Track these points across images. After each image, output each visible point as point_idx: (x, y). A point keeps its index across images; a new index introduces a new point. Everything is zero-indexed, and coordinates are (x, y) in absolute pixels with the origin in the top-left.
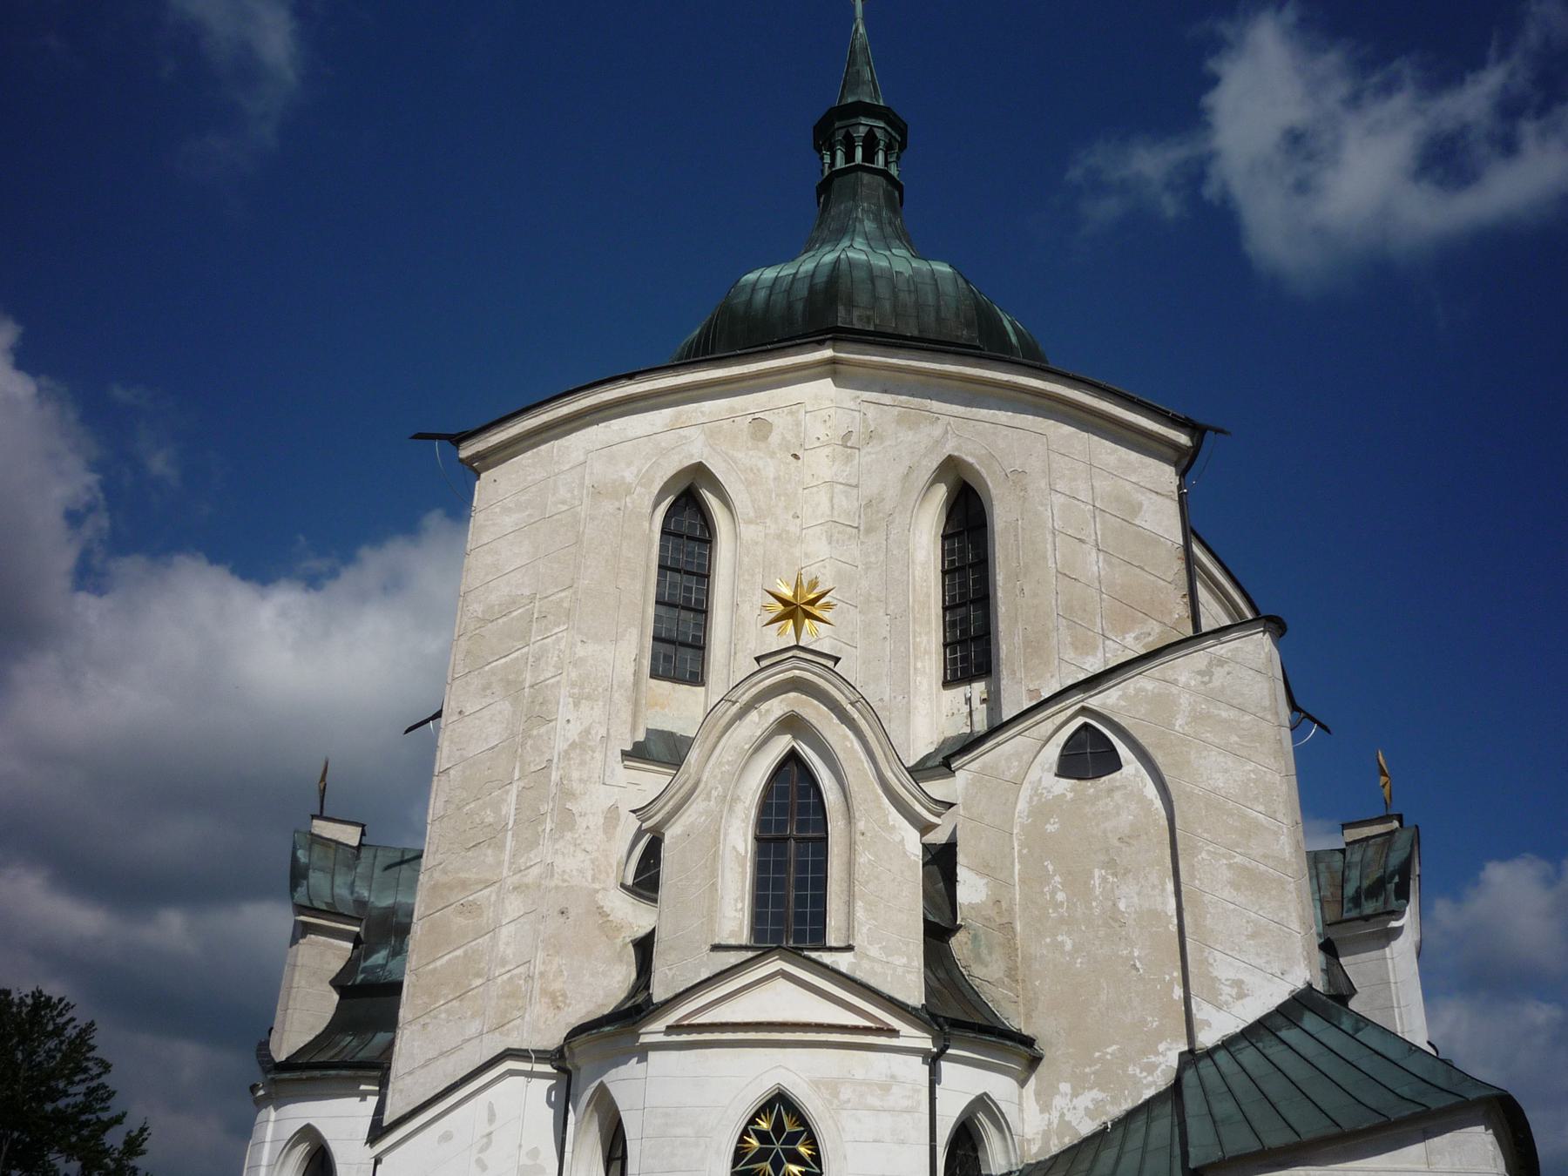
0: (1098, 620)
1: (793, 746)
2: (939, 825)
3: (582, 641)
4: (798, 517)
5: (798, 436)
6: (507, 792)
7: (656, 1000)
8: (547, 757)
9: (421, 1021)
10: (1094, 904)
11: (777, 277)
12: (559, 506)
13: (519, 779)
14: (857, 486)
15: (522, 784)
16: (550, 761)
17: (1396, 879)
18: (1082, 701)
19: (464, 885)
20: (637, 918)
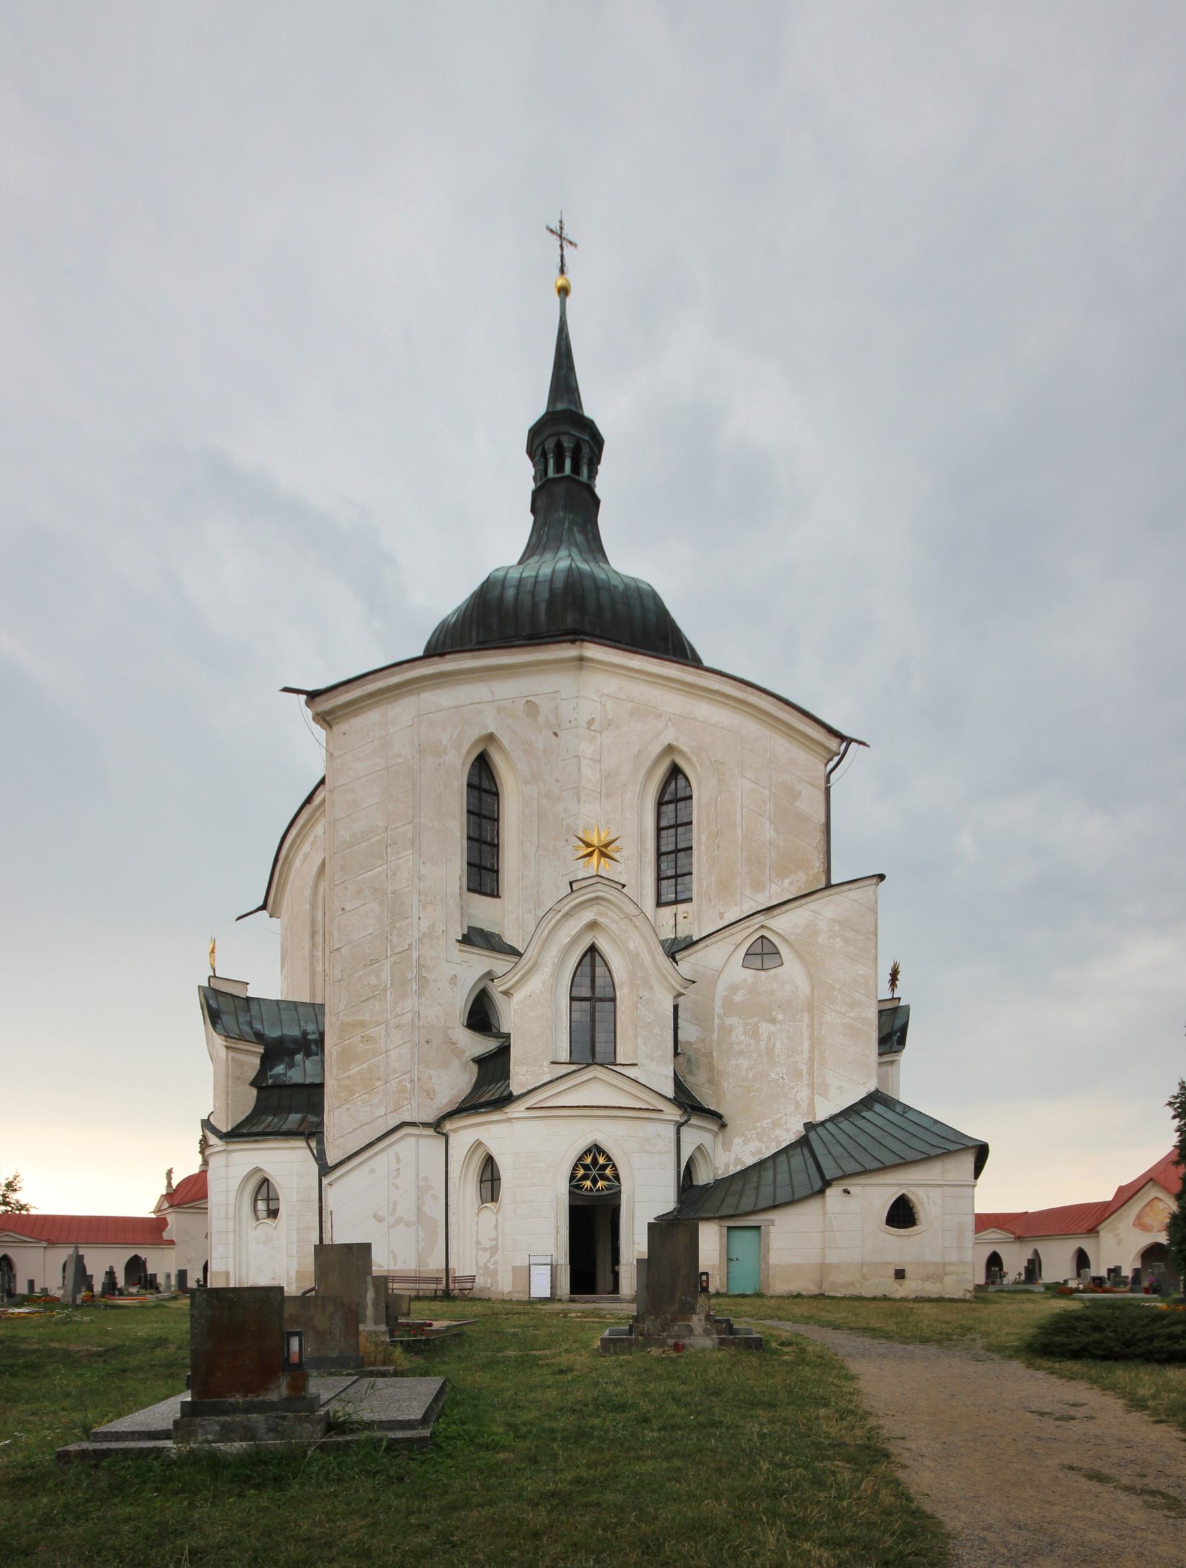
6: (384, 965)
7: (515, 1094)
9: (345, 1107)
10: (762, 1043)
11: (521, 579)
13: (391, 956)
15: (393, 959)
16: (410, 945)
19: (362, 1024)
20: (484, 1045)
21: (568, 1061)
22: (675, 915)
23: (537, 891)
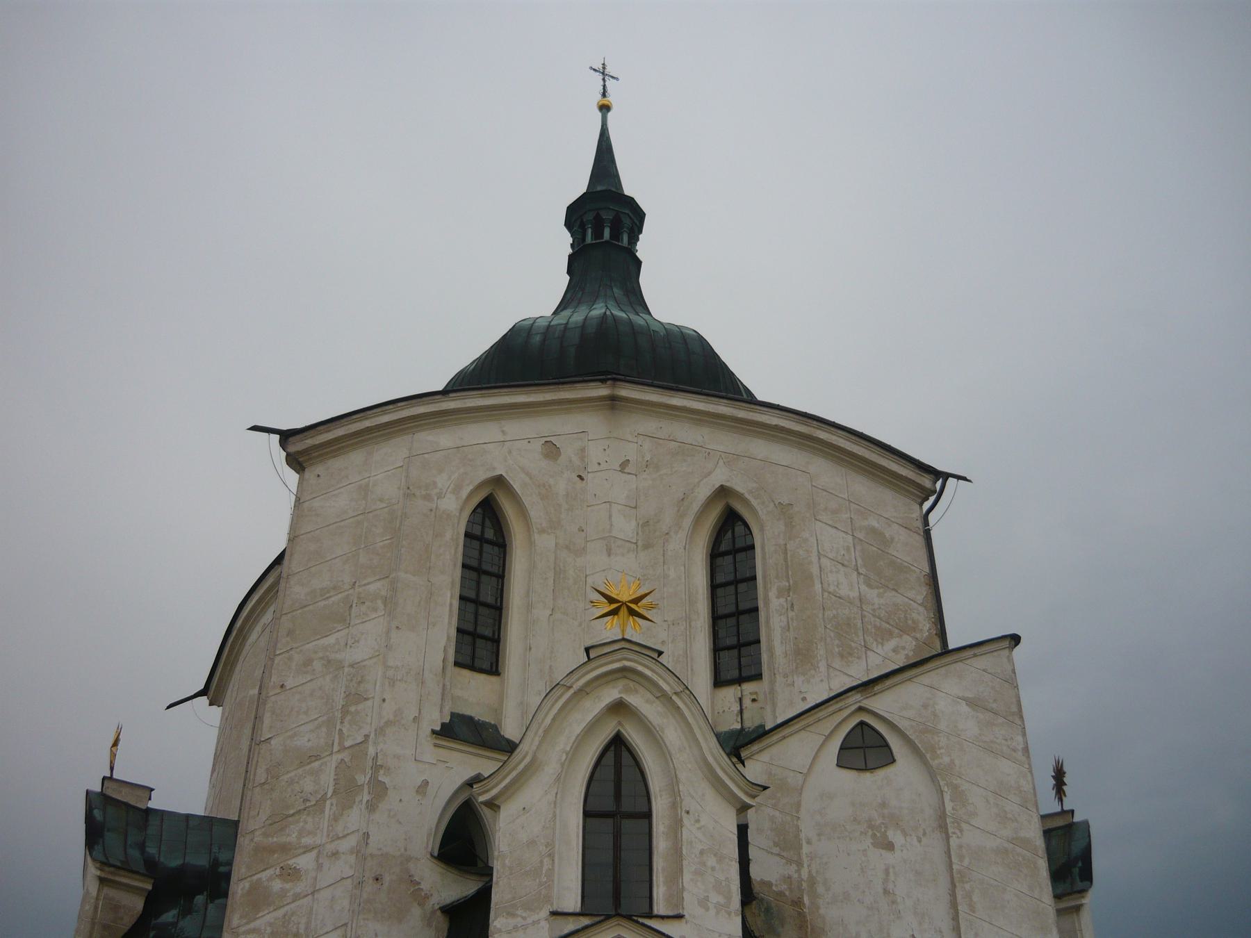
0: (861, 633)
1: (619, 730)
2: (754, 806)
3: (397, 627)
4: (583, 531)
5: (582, 459)
8: (365, 731)
11: (549, 325)
12: (378, 503)
13: (336, 752)
14: (635, 508)
15: (340, 756)
16: (367, 736)
17: (1080, 864)
18: (859, 702)
19: (285, 849)
21: (578, 910)
22: (740, 699)
23: (550, 667)
